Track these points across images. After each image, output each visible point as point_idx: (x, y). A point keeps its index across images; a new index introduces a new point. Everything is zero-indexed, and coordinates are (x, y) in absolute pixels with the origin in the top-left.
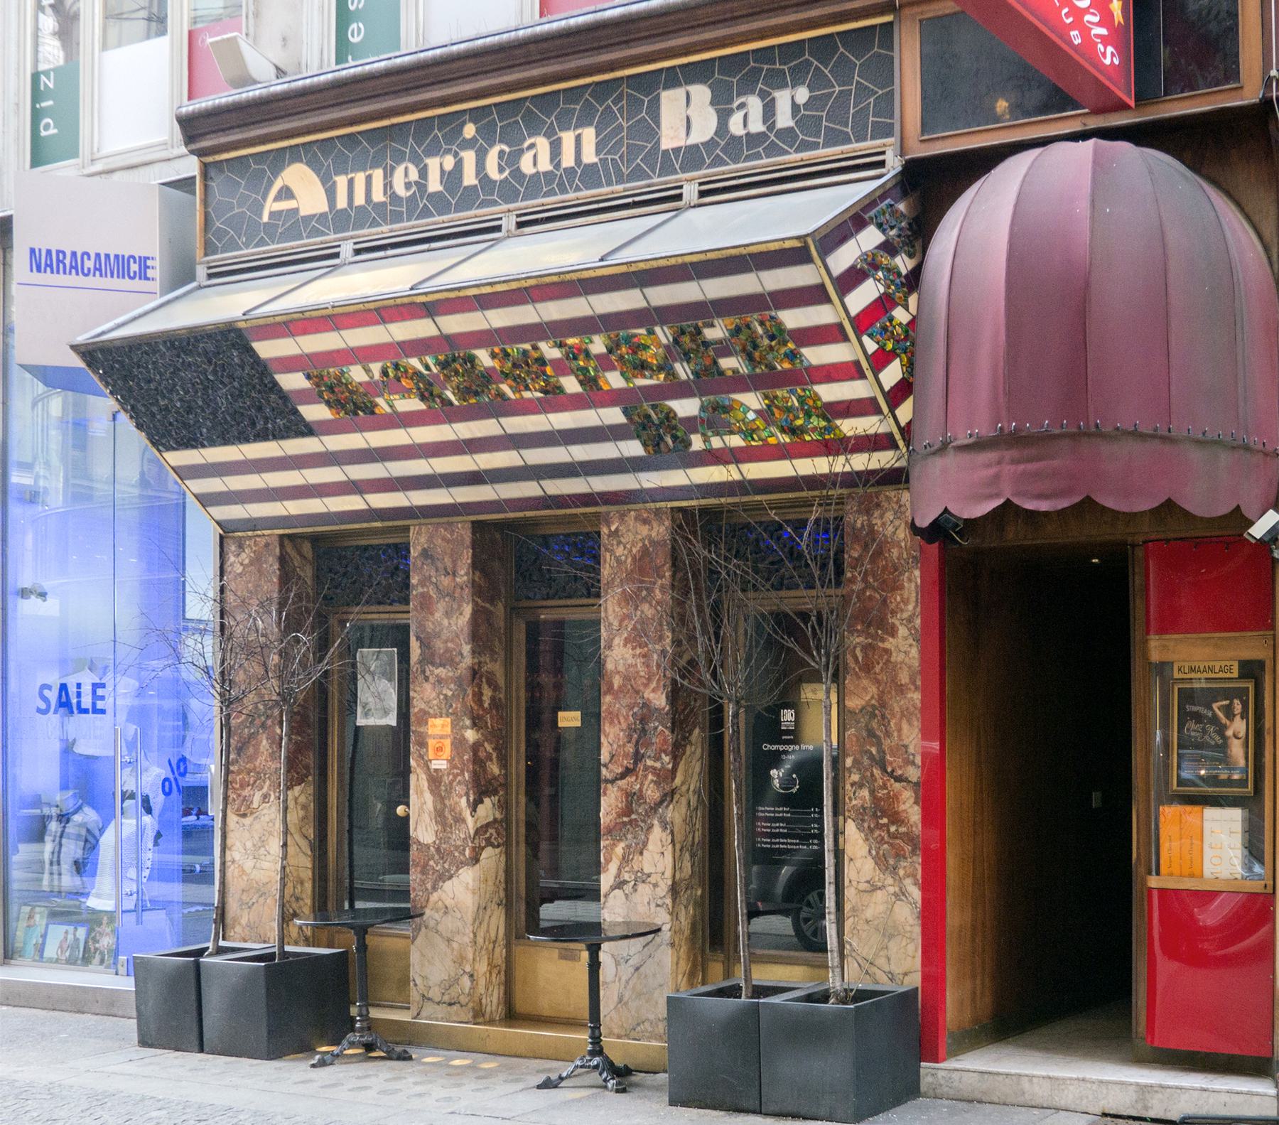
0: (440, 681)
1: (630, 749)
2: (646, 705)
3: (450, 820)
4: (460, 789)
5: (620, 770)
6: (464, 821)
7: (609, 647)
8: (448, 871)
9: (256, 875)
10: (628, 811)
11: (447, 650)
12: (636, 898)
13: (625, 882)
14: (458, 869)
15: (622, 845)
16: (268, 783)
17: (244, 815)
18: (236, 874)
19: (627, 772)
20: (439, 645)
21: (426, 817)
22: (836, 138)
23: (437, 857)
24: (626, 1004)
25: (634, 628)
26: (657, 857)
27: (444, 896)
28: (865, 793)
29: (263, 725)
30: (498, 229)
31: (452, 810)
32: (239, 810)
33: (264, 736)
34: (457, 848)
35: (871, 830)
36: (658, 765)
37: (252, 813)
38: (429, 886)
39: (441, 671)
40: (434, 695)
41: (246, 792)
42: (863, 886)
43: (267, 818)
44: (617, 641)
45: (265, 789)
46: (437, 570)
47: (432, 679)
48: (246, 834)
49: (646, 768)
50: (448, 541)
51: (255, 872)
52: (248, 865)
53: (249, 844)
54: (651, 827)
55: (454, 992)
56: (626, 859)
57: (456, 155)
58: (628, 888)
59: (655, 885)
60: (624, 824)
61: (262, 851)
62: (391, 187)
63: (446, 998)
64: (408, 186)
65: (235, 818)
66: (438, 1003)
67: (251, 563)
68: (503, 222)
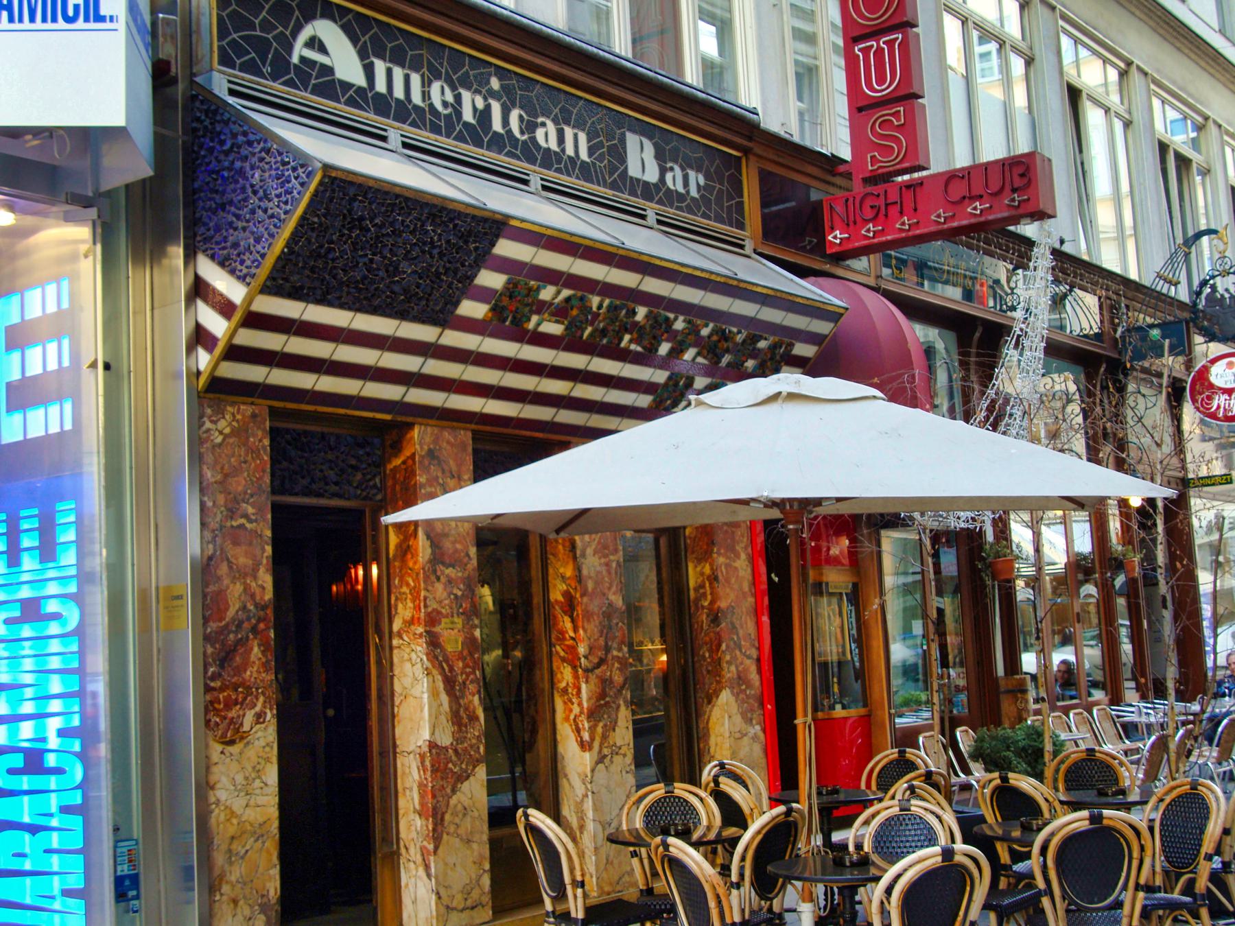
0: (450, 581)
1: (602, 642)
2: (611, 605)
3: (465, 720)
4: (472, 687)
5: (596, 661)
6: (477, 718)
7: (583, 555)
8: (466, 771)
9: (251, 815)
10: (602, 695)
11: (456, 551)
12: (613, 768)
13: (605, 756)
14: (474, 767)
15: (601, 724)
16: (261, 699)
17: (231, 742)
18: (222, 817)
19: (602, 662)
20: (447, 545)
21: (443, 719)
22: (705, 216)
23: (454, 758)
24: (612, 863)
25: (599, 543)
26: (624, 730)
27: (463, 798)
28: (733, 668)
29: (254, 630)
30: (526, 182)
31: (466, 709)
32: (224, 735)
33: (256, 643)
34: (472, 746)
35: (738, 694)
36: (620, 655)
37: (242, 738)
38: (449, 790)
39: (449, 571)
40: (445, 594)
41: (232, 714)
42: (738, 735)
43: (262, 743)
44: (589, 551)
45: (258, 709)
46: (443, 471)
47: (443, 579)
48: (235, 766)
49: (613, 657)
50: (452, 445)
51: (248, 811)
52: (238, 804)
53: (240, 778)
54: (618, 707)
55: (475, 894)
56: (604, 737)
57: (485, 99)
58: (607, 761)
59: (625, 755)
60: (601, 706)
61: (257, 783)
62: (430, 98)
63: (469, 903)
64: (445, 104)
65: (219, 747)
66: (462, 911)
67: (234, 432)
68: (531, 178)
